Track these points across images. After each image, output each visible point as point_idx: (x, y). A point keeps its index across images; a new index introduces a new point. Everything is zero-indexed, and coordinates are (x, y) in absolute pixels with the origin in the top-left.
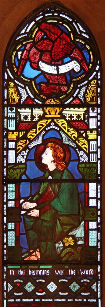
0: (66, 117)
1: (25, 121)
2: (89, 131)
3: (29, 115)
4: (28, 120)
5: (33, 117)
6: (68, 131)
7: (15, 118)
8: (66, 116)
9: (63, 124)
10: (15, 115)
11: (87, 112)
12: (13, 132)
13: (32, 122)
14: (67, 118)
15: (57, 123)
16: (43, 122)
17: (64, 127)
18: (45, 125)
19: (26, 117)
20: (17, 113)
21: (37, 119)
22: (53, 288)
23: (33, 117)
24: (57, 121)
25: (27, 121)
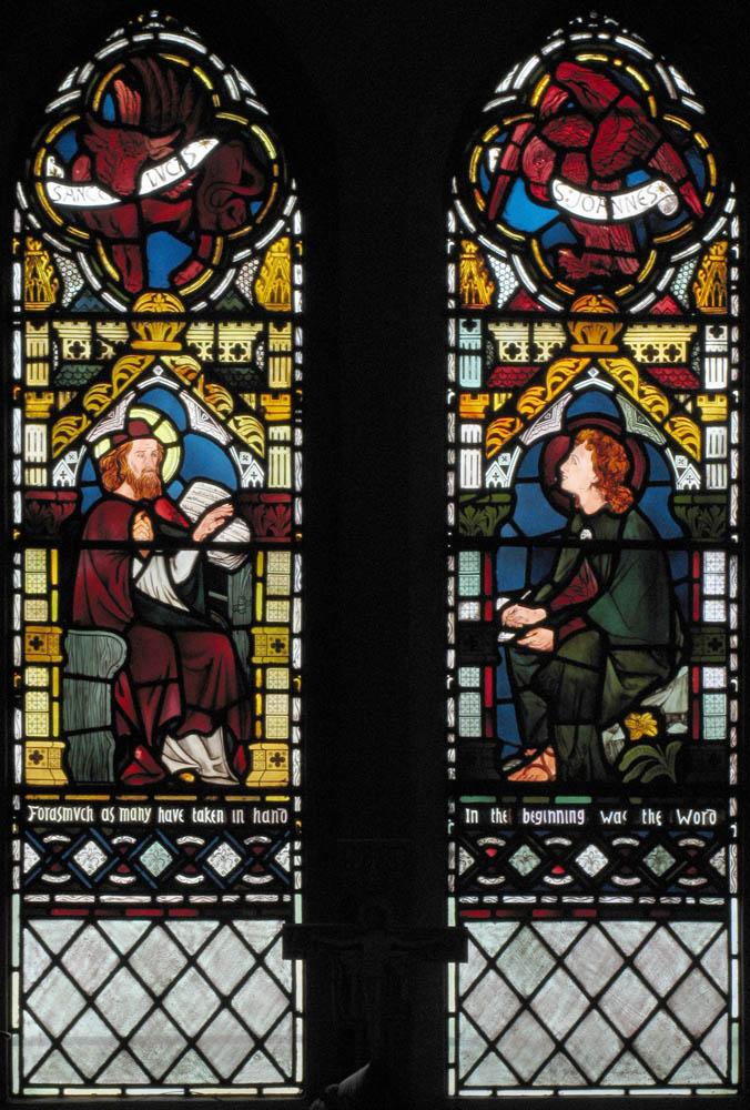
0: (634, 352)
1: (509, 360)
2: (704, 397)
3: (523, 343)
4: (520, 358)
5: (533, 350)
6: (642, 394)
7: (482, 353)
8: (633, 348)
9: (627, 373)
10: (479, 342)
11: (698, 339)
12: (474, 393)
13: (531, 364)
14: (639, 357)
15: (607, 369)
16: (564, 365)
17: (630, 384)
18: (571, 375)
19: (513, 351)
20: (487, 336)
21: (546, 355)
22: (595, 866)
23: (533, 350)
24: (608, 363)
25: (516, 360)
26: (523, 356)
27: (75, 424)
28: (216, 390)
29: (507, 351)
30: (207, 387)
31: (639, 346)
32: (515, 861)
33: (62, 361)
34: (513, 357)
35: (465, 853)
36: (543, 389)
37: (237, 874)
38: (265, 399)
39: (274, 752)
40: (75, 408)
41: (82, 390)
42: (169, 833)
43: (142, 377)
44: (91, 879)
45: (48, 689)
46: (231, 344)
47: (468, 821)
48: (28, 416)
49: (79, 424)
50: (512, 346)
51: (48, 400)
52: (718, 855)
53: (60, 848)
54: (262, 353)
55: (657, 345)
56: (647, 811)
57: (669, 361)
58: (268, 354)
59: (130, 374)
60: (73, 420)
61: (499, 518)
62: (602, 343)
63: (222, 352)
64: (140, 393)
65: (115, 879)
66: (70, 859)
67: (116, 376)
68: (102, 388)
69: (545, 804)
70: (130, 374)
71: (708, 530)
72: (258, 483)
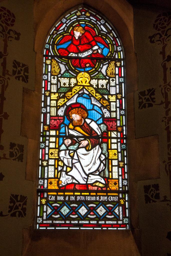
0: (93, 86)
1: (64, 86)
2: (110, 96)
3: (67, 82)
4: (66, 86)
5: (70, 84)
6: (96, 95)
7: (57, 84)
8: (93, 85)
9: (92, 91)
10: (56, 82)
11: (109, 83)
12: (55, 93)
13: (70, 87)
14: (94, 87)
15: (88, 89)
16: (77, 88)
17: (93, 93)
18: (78, 90)
19: (65, 84)
20: (58, 81)
21: (72, 85)
22: (102, 212)
23: (70, 84)
24: (88, 88)
25: (65, 86)
26: (67, 85)
27: (63, 101)
28: (98, 95)
29: (63, 84)
30: (96, 94)
31: (72, 83)
32: (80, 210)
33: (61, 87)
34: (64, 85)
35: (49, 208)
36: (71, 93)
37: (86, 215)
38: (109, 96)
39: (114, 182)
40: (64, 97)
41: (65, 93)
42: (103, 204)
43: (80, 91)
44: (65, 216)
45: (54, 165)
46: (73, 83)
47: (71, 200)
48: (52, 99)
49: (64, 101)
50: (64, 83)
51: (57, 95)
52: (117, 209)
53: (111, 208)
54: (109, 86)
55: (66, 83)
56: (71, 197)
57: (102, 88)
58: (110, 86)
59: (77, 90)
60: (62, 100)
61: (166, 127)
62: (85, 83)
63: (71, 84)
64: (79, 94)
65: (108, 216)
66: (78, 211)
67: (73, 90)
68: (70, 93)
69: (105, 195)
70: (77, 90)
71: (112, 126)
72: (108, 116)
